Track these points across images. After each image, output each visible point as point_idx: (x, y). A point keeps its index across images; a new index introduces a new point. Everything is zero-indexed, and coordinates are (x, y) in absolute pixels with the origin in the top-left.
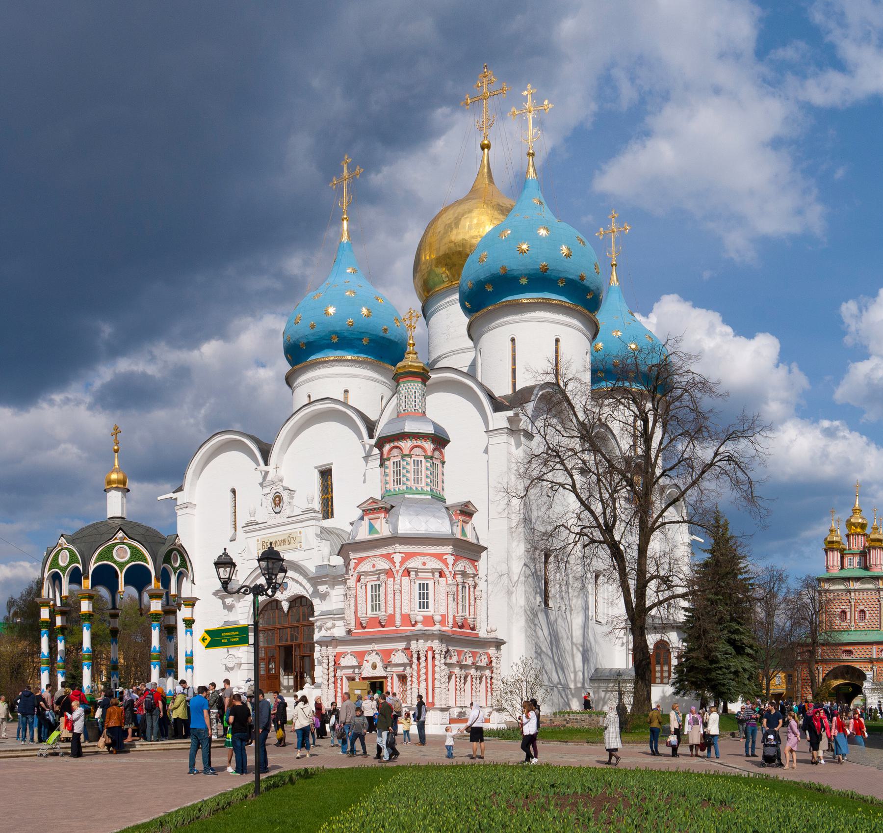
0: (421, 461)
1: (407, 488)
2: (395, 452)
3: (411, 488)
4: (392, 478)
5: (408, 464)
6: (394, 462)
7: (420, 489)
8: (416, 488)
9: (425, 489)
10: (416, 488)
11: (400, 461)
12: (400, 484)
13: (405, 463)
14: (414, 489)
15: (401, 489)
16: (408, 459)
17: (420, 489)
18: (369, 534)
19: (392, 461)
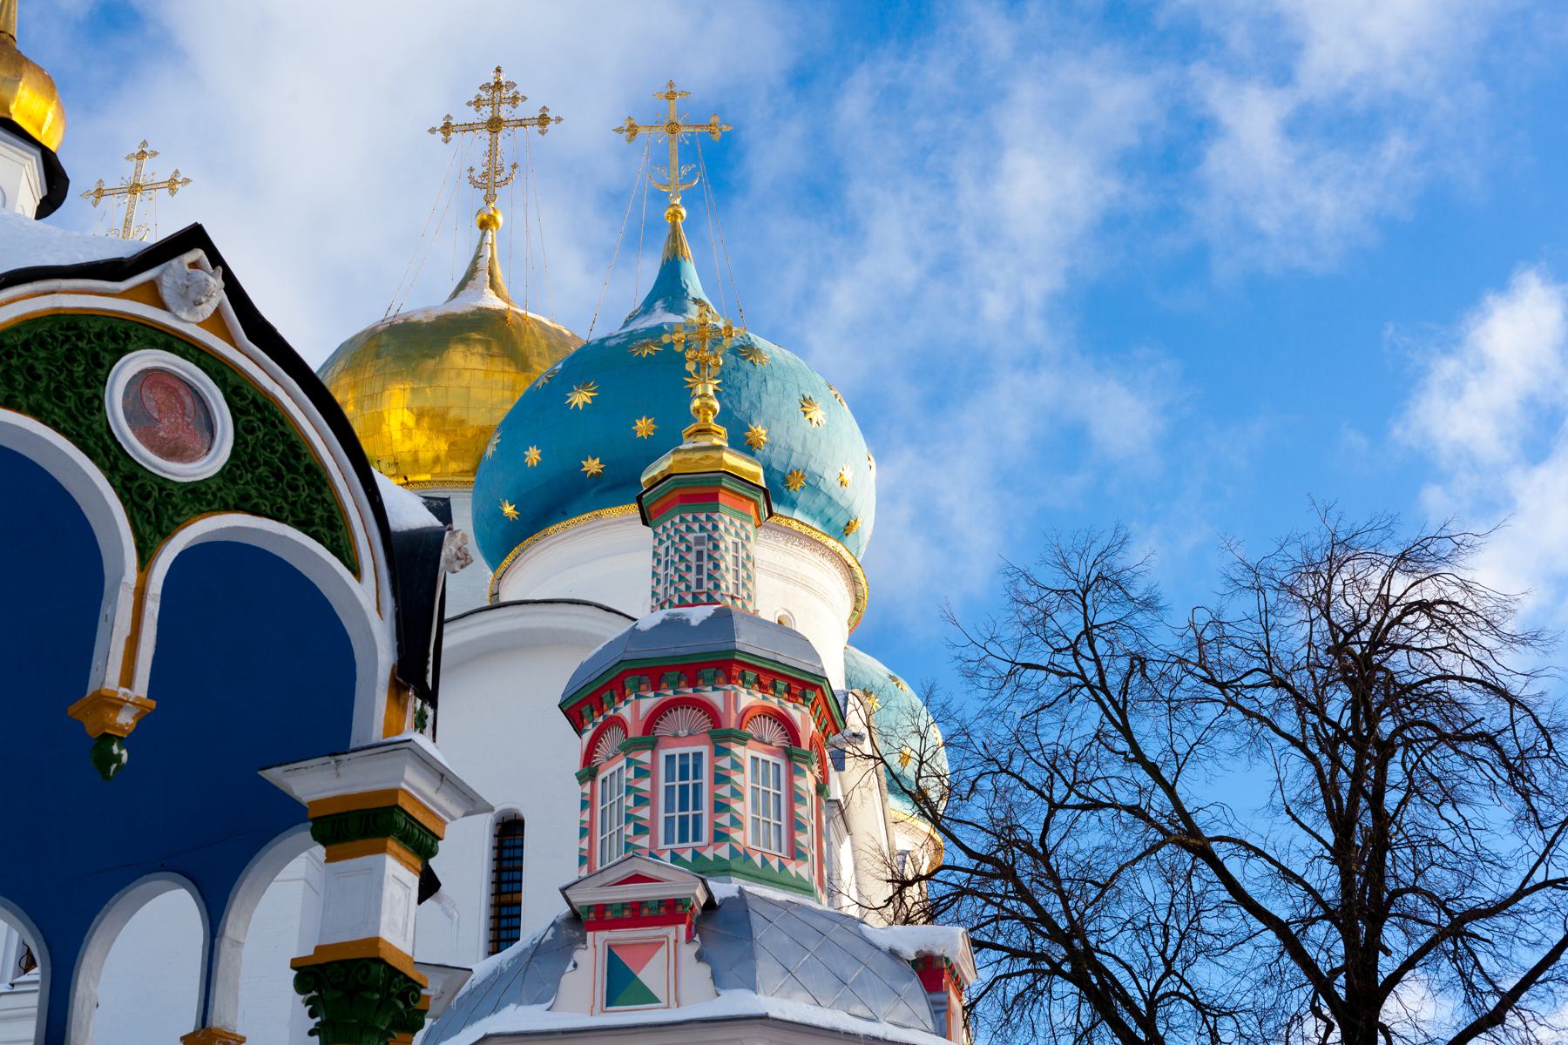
0: (778, 766)
1: (734, 852)
2: (681, 720)
3: (747, 857)
4: (662, 815)
5: (737, 766)
6: (670, 758)
7: (775, 864)
8: (765, 862)
9: (792, 867)
10: (765, 862)
11: (698, 756)
12: (697, 837)
13: (725, 763)
14: (757, 859)
15: (709, 854)
16: (737, 750)
17: (775, 864)
18: (611, 1001)
19: (662, 755)
